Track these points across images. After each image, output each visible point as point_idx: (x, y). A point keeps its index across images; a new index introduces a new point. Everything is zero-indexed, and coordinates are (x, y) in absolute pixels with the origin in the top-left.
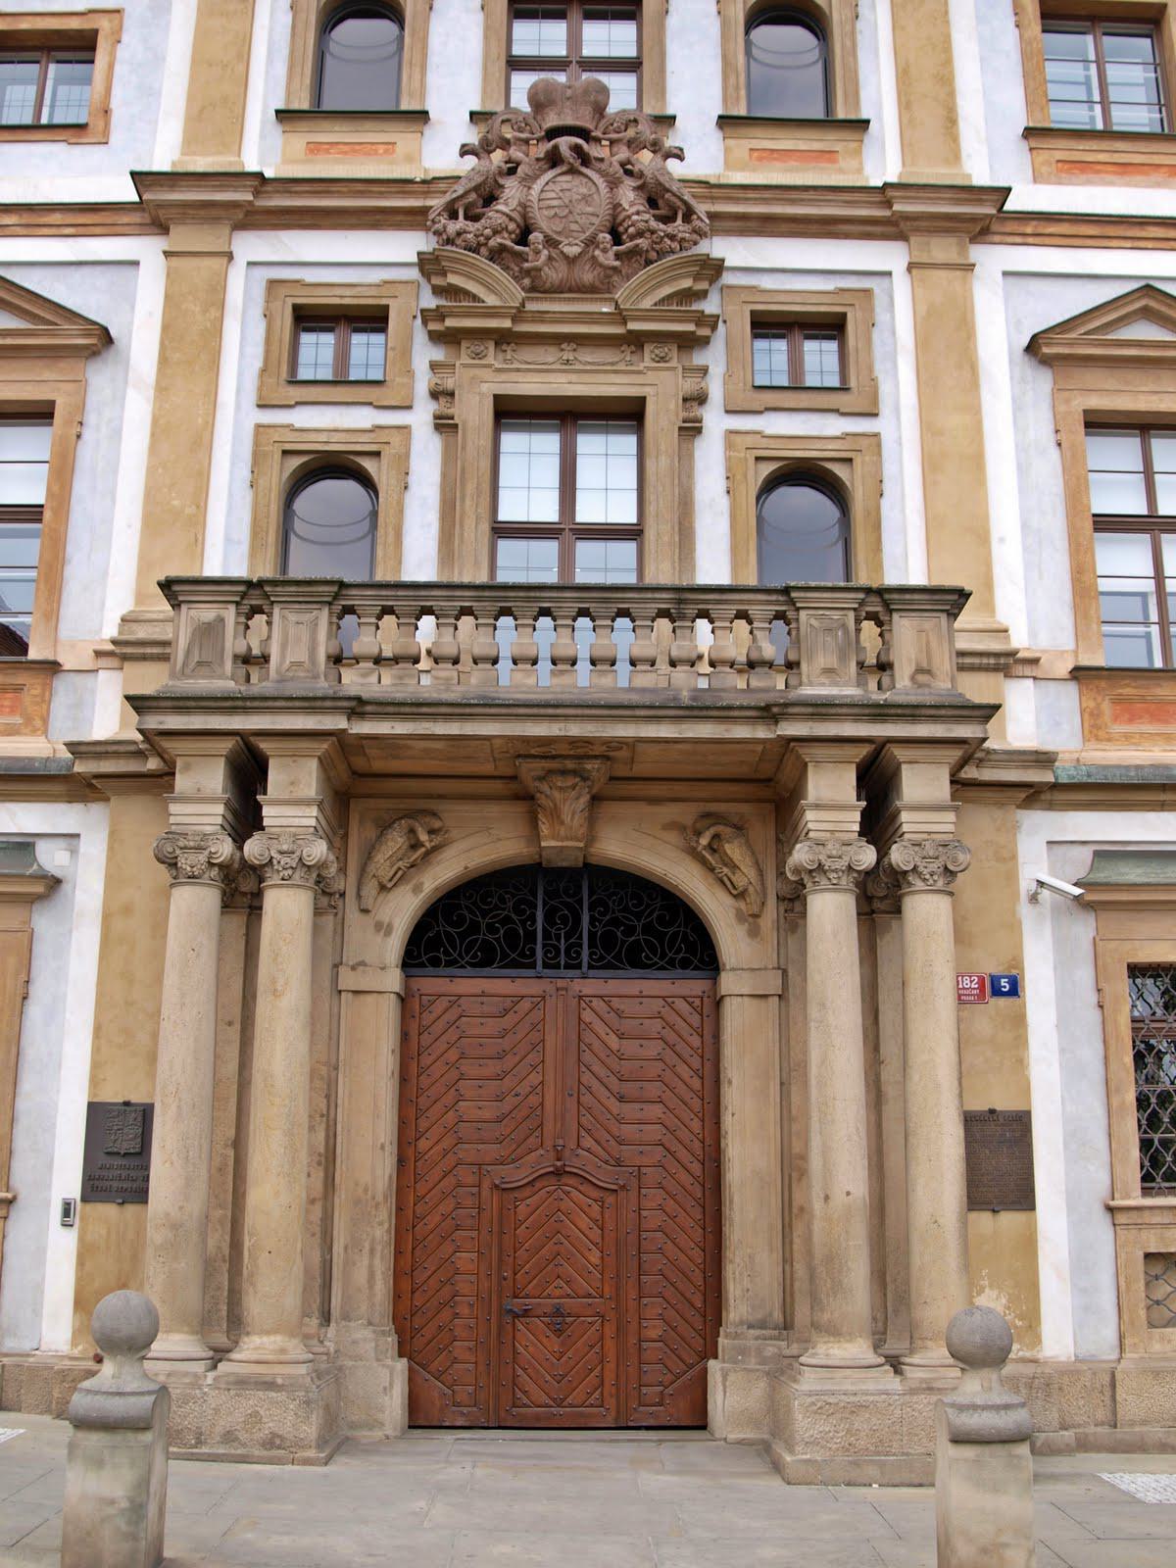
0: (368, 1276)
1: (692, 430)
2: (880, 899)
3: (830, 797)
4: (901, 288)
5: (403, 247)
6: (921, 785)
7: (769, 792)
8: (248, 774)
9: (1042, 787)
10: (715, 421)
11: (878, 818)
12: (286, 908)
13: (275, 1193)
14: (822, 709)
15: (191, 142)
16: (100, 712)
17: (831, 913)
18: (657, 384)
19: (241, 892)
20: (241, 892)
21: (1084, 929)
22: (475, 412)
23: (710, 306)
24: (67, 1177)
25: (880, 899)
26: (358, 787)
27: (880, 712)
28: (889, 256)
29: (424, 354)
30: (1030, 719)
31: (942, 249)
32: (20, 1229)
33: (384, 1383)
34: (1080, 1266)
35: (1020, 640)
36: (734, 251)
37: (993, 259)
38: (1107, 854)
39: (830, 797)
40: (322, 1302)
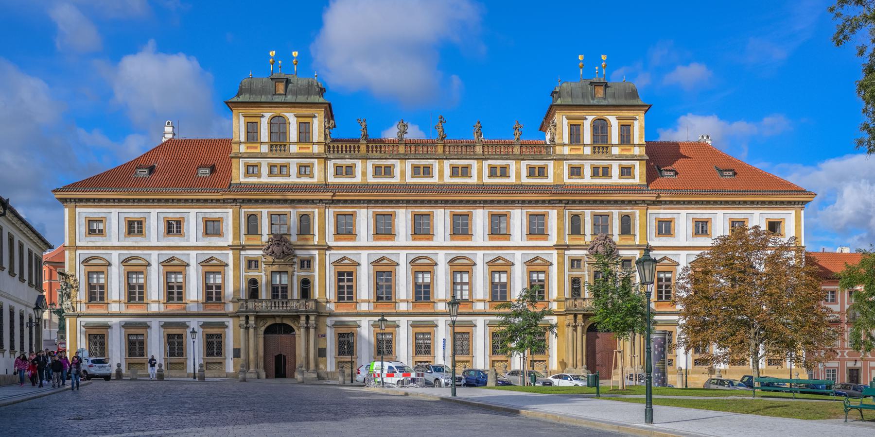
0: (261, 364)
1: (293, 275)
2: (307, 329)
3: (303, 318)
4: (317, 256)
5: (261, 252)
6: (312, 318)
7: (297, 318)
8: (247, 317)
12: (251, 331)
13: (252, 356)
14: (302, 311)
15: (234, 239)
16: (230, 308)
17: (302, 330)
18: (289, 269)
19: (247, 328)
20: (247, 328)
21: (333, 329)
22: (269, 274)
23: (295, 260)
24: (231, 356)
25: (307, 329)
26: (258, 318)
27: (306, 312)
28: (316, 252)
29: (263, 266)
31: (322, 252)
32: (227, 361)
33: (263, 374)
36: (298, 252)
37: (328, 253)
39: (303, 318)
40: (257, 366)
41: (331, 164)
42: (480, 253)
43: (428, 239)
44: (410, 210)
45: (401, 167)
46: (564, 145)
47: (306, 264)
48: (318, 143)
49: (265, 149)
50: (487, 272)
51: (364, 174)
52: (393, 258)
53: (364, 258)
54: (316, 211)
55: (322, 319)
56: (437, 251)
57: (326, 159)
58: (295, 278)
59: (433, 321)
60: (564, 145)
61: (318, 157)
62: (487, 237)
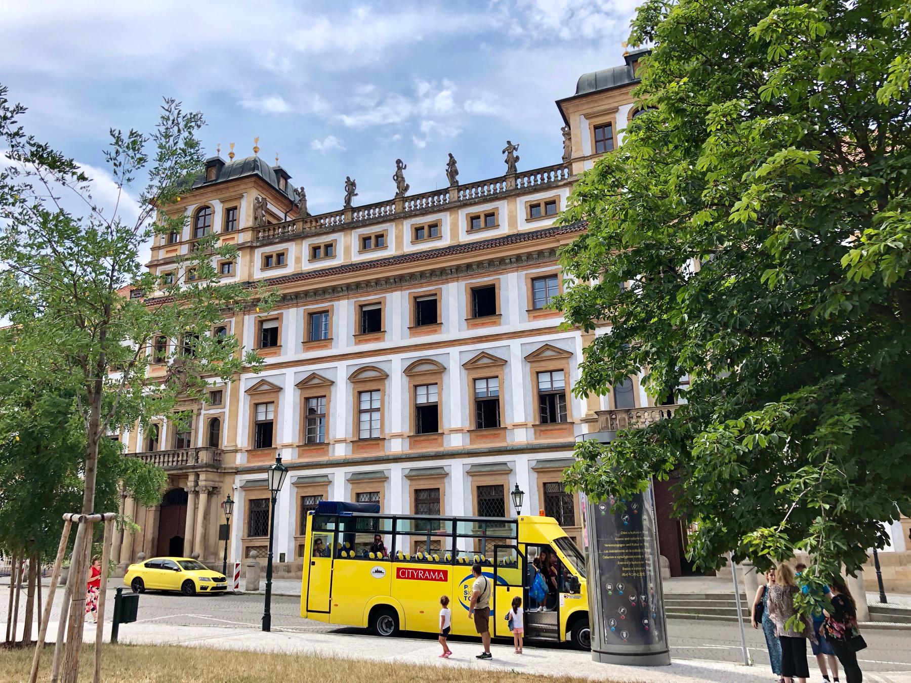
1: (200, 414)
9: (238, 471)
10: (203, 412)
11: (197, 484)
18: (195, 407)
21: (243, 493)
30: (240, 460)
34: (237, 548)
35: (239, 446)
38: (248, 482)
41: (258, 254)
42: (454, 351)
43: (378, 339)
44: (354, 300)
45: (346, 242)
46: (584, 158)
47: (216, 396)
48: (243, 230)
49: (184, 250)
50: (465, 380)
51: (298, 260)
52: (328, 375)
53: (289, 379)
54: (233, 320)
55: (228, 479)
56: (389, 357)
57: (252, 248)
58: (202, 418)
59: (382, 472)
60: (584, 158)
61: (241, 247)
62: (465, 324)
